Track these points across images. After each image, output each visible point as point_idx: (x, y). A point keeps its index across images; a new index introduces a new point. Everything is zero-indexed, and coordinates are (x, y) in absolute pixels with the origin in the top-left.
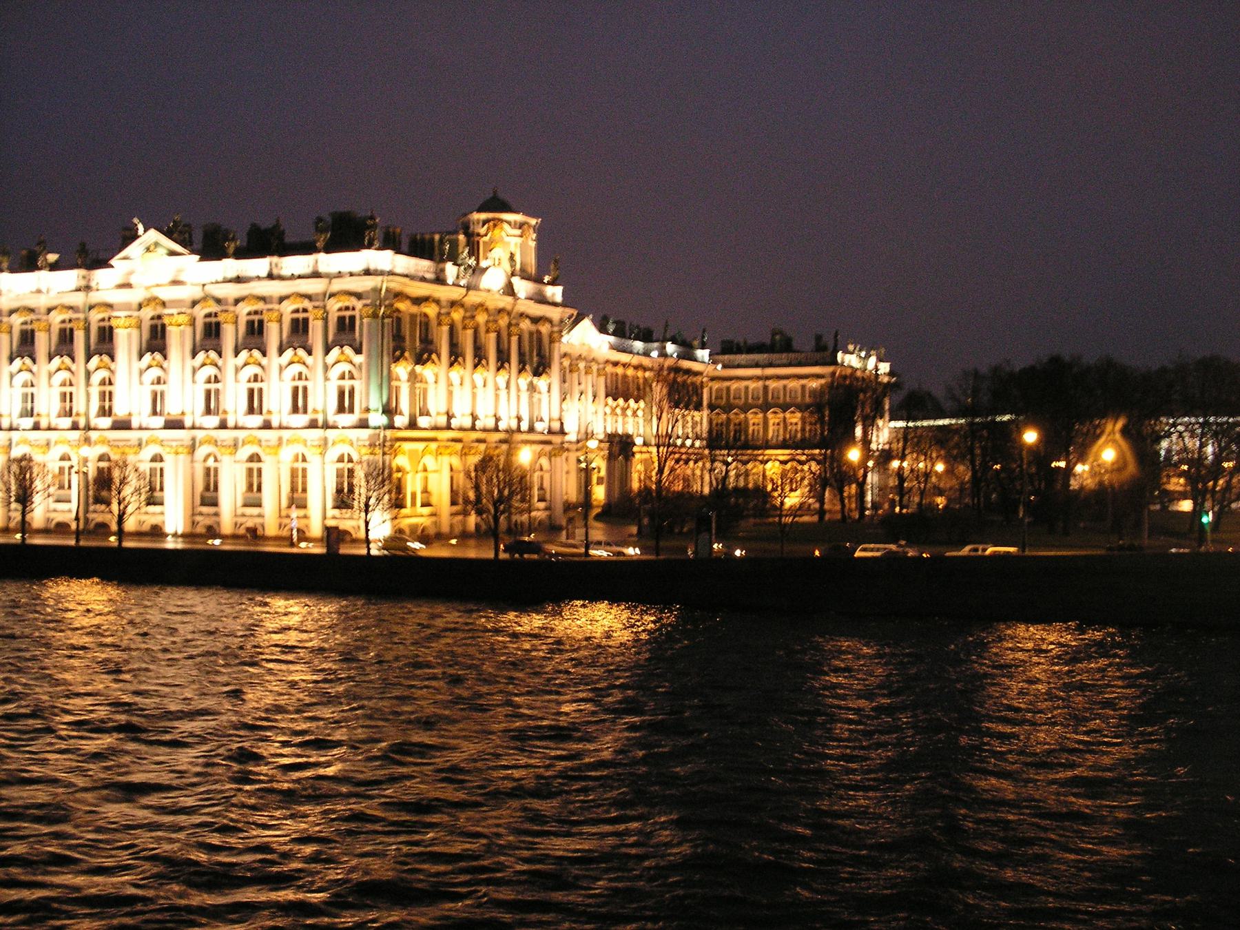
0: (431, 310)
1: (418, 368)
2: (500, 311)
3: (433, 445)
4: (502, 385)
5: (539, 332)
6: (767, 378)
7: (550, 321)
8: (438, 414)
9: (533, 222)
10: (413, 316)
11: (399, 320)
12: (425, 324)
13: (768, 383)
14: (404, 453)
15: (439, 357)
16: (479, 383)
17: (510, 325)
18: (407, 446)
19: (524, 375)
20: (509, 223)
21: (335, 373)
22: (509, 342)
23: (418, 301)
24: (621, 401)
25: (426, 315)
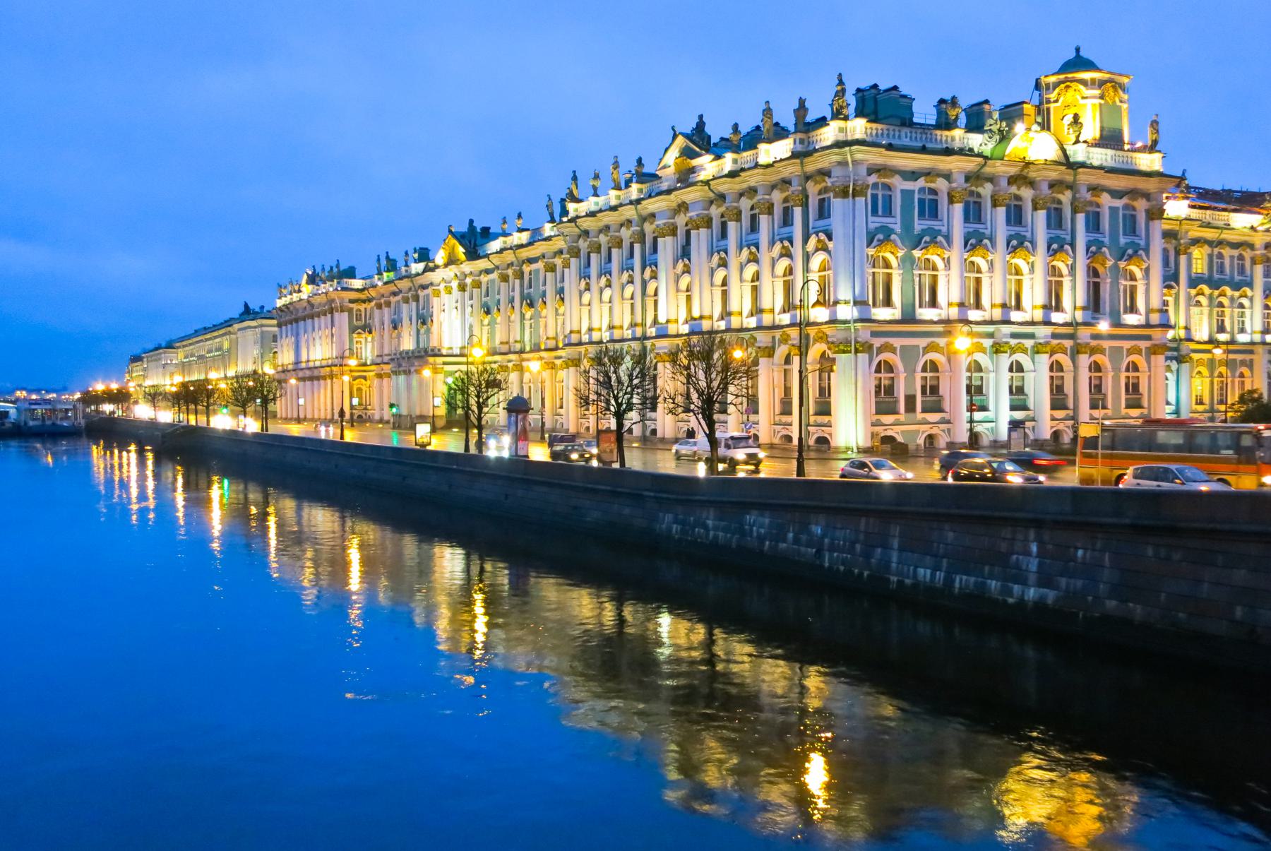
0: (941, 184)
4: (1065, 271)
10: (907, 194)
11: (889, 200)
14: (893, 350)
16: (1024, 267)
18: (897, 342)
20: (1083, 82)
22: (1073, 220)
23: (913, 175)
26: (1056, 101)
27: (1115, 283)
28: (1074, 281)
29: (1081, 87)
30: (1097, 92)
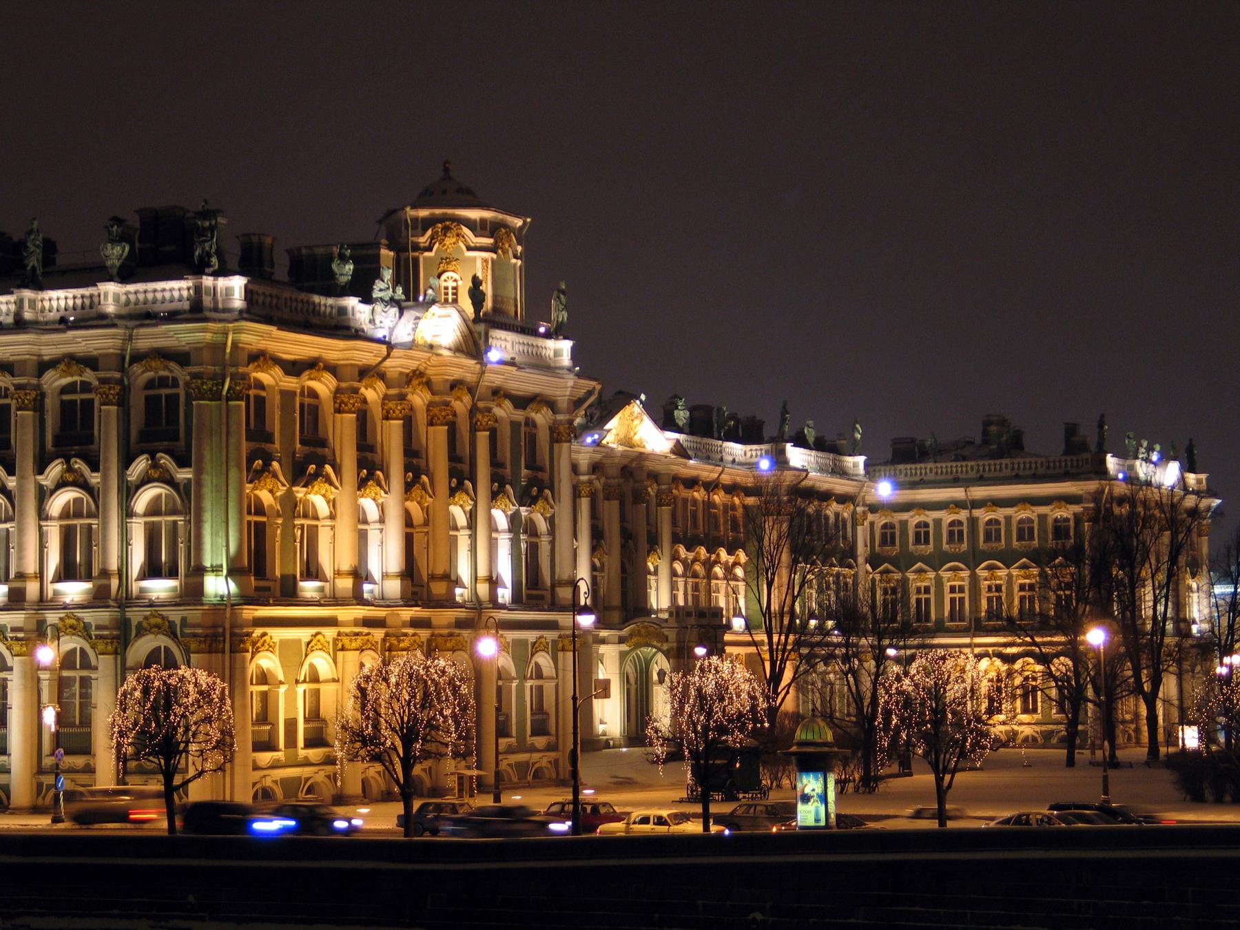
0: (324, 386)
1: (300, 492)
2: (455, 385)
3: (329, 633)
4: (462, 520)
5: (530, 423)
6: (976, 504)
7: (551, 404)
8: (338, 573)
9: (518, 223)
10: (287, 395)
11: (260, 402)
12: (311, 411)
13: (977, 513)
14: (271, 648)
15: (337, 470)
17: (473, 410)
18: (278, 634)
19: (503, 501)
21: (142, 501)
23: (294, 368)
24: (703, 551)
25: (313, 394)
26: (430, 249)
27: (515, 543)
28: (473, 538)
29: (466, 230)
30: (491, 241)
